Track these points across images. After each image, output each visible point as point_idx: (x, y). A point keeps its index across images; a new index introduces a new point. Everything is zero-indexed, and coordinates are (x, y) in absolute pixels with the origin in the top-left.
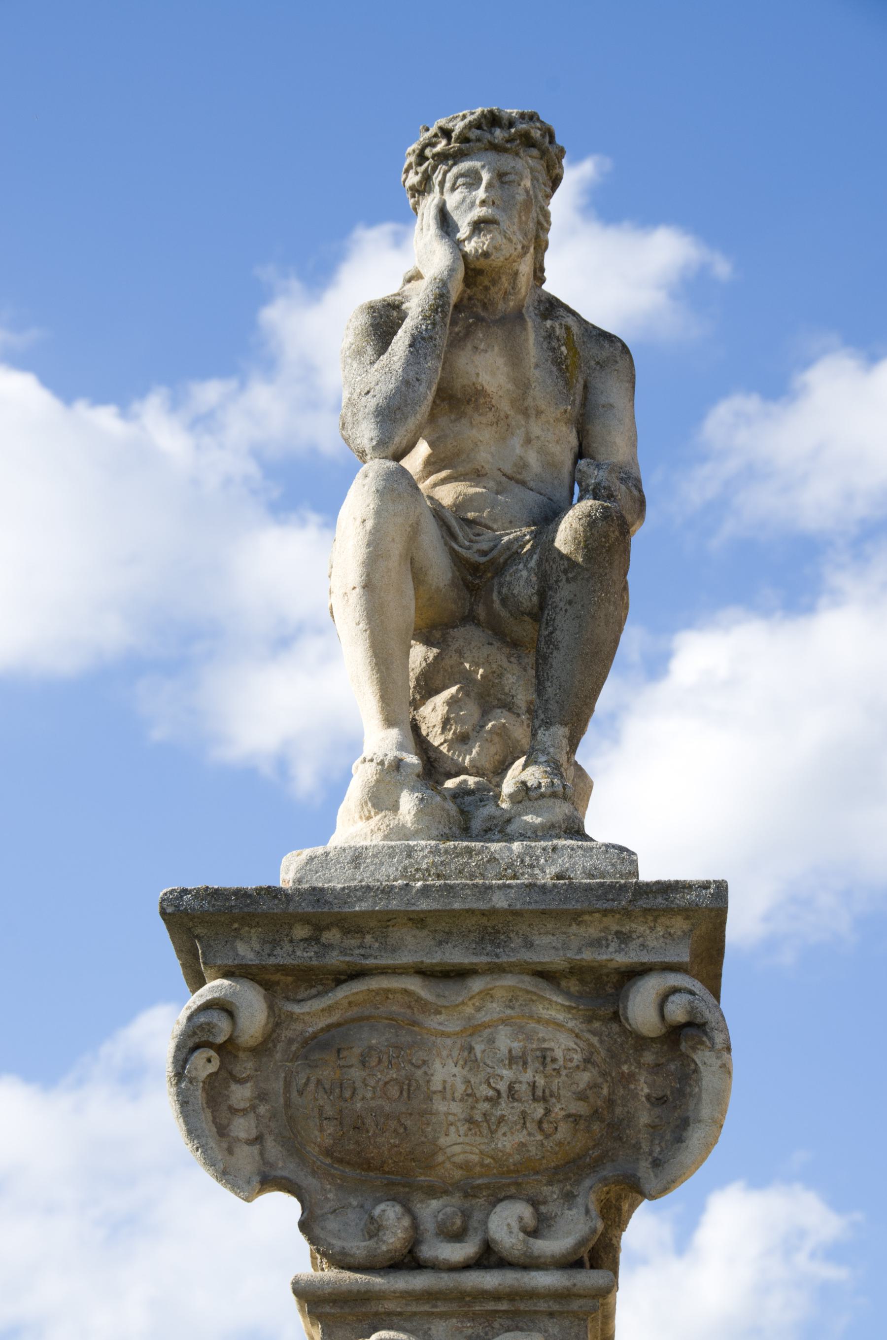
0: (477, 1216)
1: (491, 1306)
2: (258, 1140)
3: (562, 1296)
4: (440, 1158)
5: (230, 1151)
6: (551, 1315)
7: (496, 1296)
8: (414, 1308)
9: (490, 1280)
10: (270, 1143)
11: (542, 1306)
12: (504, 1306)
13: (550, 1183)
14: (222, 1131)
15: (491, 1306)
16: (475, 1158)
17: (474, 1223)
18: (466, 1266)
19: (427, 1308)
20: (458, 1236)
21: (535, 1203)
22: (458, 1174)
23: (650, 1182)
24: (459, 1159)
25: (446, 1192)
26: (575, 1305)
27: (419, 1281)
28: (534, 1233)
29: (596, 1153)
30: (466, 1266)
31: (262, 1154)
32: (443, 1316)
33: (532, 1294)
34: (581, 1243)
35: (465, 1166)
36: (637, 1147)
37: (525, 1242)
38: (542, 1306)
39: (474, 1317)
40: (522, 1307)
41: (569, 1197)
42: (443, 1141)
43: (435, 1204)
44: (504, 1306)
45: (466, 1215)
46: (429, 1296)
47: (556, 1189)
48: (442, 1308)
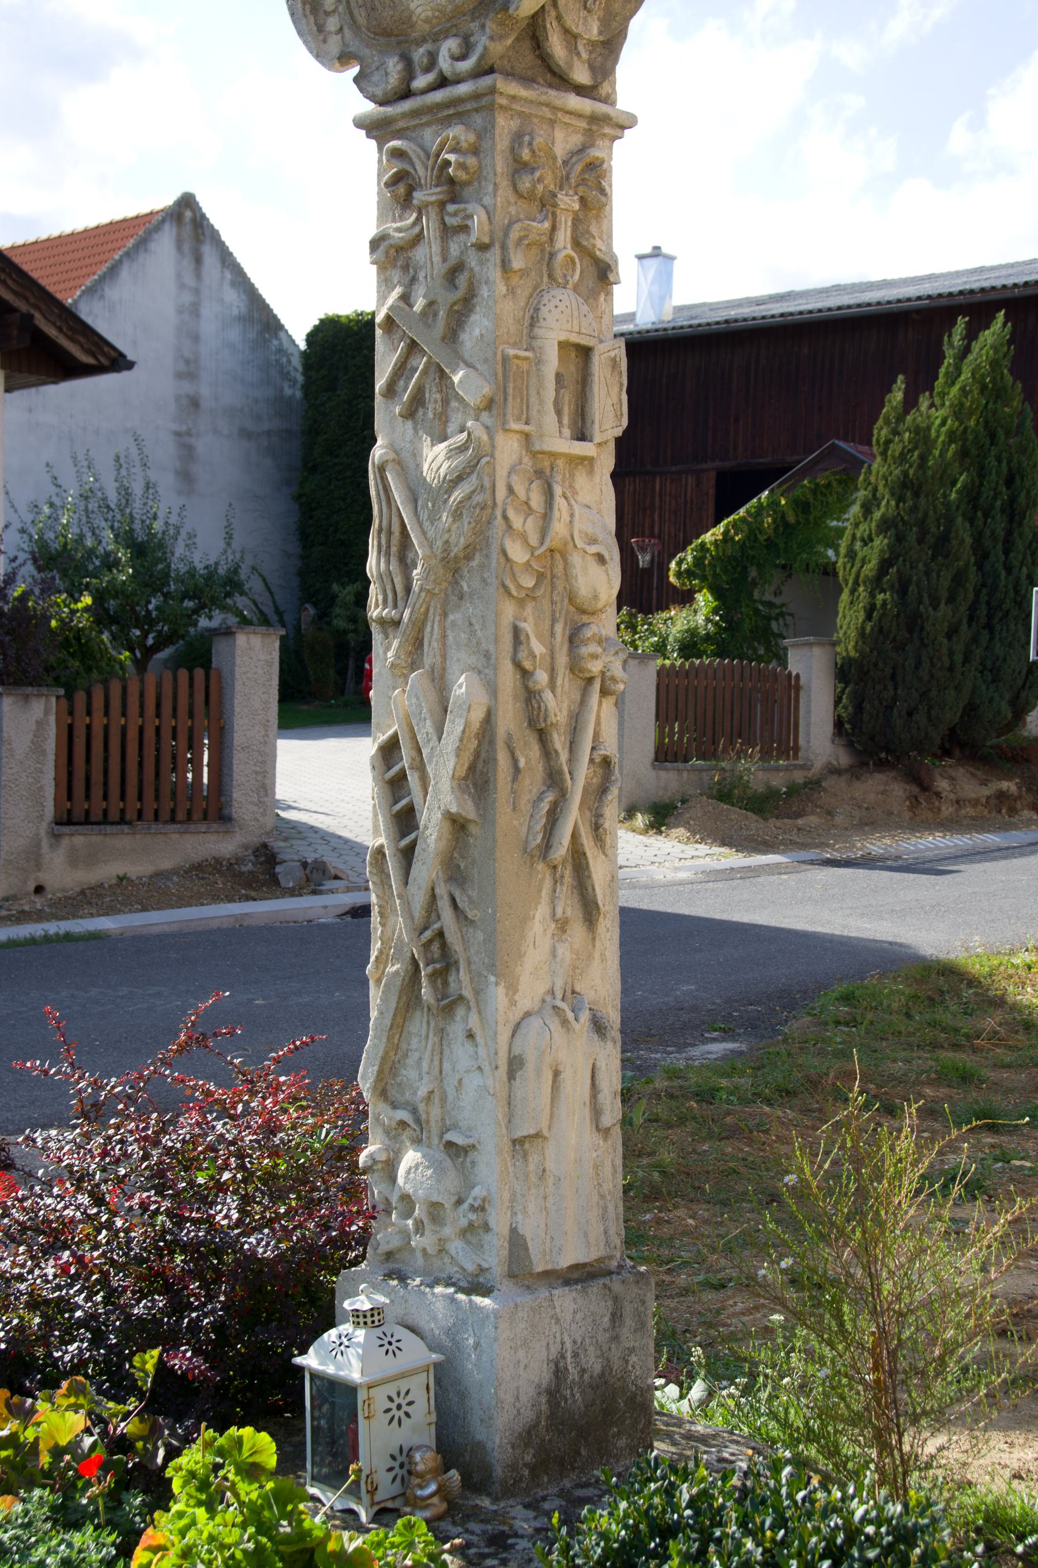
1: (446, 113)
2: (341, 30)
3: (476, 96)
4: (414, 19)
5: (325, 41)
6: (477, 110)
10: (346, 30)
11: (469, 106)
12: (451, 111)
13: (473, 20)
14: (320, 28)
15: (446, 113)
16: (429, 13)
19: (417, 122)
24: (423, 16)
26: (484, 101)
31: (343, 38)
32: (428, 124)
35: (427, 21)
37: (452, 65)
38: (469, 106)
40: (460, 109)
42: (412, 6)
44: (451, 111)
46: (415, 113)
47: (477, 24)
48: (424, 119)
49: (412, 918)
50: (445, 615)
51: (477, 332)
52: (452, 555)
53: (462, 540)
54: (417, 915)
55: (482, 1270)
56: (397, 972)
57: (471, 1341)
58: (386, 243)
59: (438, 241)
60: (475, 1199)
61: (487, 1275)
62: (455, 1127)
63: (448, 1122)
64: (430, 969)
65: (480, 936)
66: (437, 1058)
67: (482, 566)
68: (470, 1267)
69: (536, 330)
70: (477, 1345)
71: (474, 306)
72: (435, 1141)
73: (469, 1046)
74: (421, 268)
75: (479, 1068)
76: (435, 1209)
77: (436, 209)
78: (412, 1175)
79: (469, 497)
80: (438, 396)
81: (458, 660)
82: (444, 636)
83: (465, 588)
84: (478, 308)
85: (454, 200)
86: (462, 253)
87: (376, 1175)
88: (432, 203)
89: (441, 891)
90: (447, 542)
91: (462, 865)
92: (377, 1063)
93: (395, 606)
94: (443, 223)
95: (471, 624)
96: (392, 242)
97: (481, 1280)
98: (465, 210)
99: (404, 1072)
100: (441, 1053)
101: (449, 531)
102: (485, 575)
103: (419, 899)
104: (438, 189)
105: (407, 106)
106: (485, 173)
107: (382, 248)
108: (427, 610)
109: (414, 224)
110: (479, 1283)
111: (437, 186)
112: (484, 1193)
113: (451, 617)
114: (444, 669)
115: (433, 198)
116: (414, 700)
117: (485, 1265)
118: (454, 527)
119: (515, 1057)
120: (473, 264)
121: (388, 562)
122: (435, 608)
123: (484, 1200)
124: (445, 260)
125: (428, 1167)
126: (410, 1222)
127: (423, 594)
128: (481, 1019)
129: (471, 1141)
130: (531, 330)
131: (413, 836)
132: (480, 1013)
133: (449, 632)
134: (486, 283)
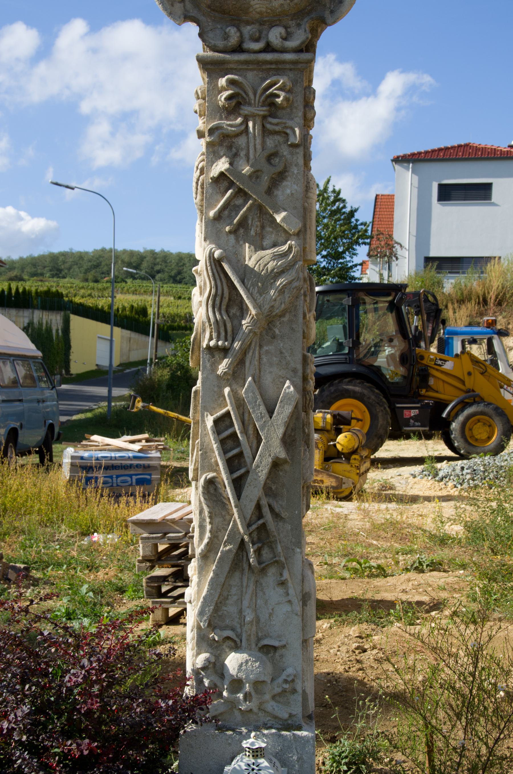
0: (265, 32)
1: (268, 66)
3: (295, 63)
4: (251, 10)
6: (291, 70)
7: (271, 63)
8: (240, 67)
9: (269, 56)
11: (288, 66)
12: (273, 66)
13: (292, 20)
15: (268, 66)
16: (264, 10)
17: (263, 35)
18: (260, 51)
19: (245, 67)
20: (257, 40)
21: (286, 27)
22: (258, 16)
23: (329, 19)
24: (258, 10)
25: (253, 23)
26: (299, 66)
27: (243, 57)
28: (285, 39)
29: (310, 8)
30: (260, 51)
31: (184, 7)
32: (251, 70)
33: (284, 62)
34: (303, 43)
35: (260, 13)
36: (325, 5)
37: (282, 42)
38: (288, 66)
39: (263, 70)
40: (280, 67)
41: (299, 25)
42: (252, 3)
43: (249, 28)
44: (273, 66)
45: (260, 32)
46: (246, 62)
47: (294, 22)
48: (251, 67)
49: (245, 518)
50: (261, 346)
51: (288, 191)
52: (274, 313)
53: (283, 306)
54: (167, 518)
55: (291, 716)
56: (230, 550)
57: (295, 758)
58: (220, 131)
59: (260, 137)
60: (288, 676)
61: (294, 719)
62: (267, 636)
63: (260, 634)
64: (256, 546)
65: (289, 527)
66: (254, 598)
67: (291, 321)
68: (286, 716)
69: (309, 193)
70: (299, 759)
71: (286, 177)
72: (254, 646)
73: (280, 590)
74: (242, 149)
75: (290, 602)
76: (257, 684)
77: (261, 119)
78: (244, 668)
79: (290, 283)
80: (259, 223)
81: (270, 372)
82: (260, 358)
83: (277, 332)
84: (289, 178)
85: (273, 115)
86: (276, 146)
87: (209, 670)
88: (259, 115)
89: (264, 502)
90: (273, 307)
91: (274, 488)
92: (213, 604)
93: (226, 340)
94: (263, 126)
95: (281, 353)
96: (224, 131)
97: (290, 722)
98: (285, 123)
99: (225, 608)
100: (256, 596)
101: (275, 300)
102: (294, 326)
103: (250, 507)
104: (264, 108)
105: (237, 57)
106: (296, 105)
107: (217, 133)
108: (251, 344)
109: (241, 124)
110: (289, 724)
111: (262, 106)
112: (295, 672)
113: (265, 348)
114: (260, 377)
115: (262, 113)
116: (250, 394)
117: (294, 713)
118: (278, 299)
119: (306, 593)
120: (285, 153)
121: (220, 314)
122: (256, 342)
123: (295, 676)
124: (263, 149)
125: (256, 661)
126: (241, 696)
127: (251, 334)
128: (290, 573)
129: (283, 643)
130: (307, 194)
131: (242, 471)
132: (289, 571)
133: (263, 356)
134: (296, 165)
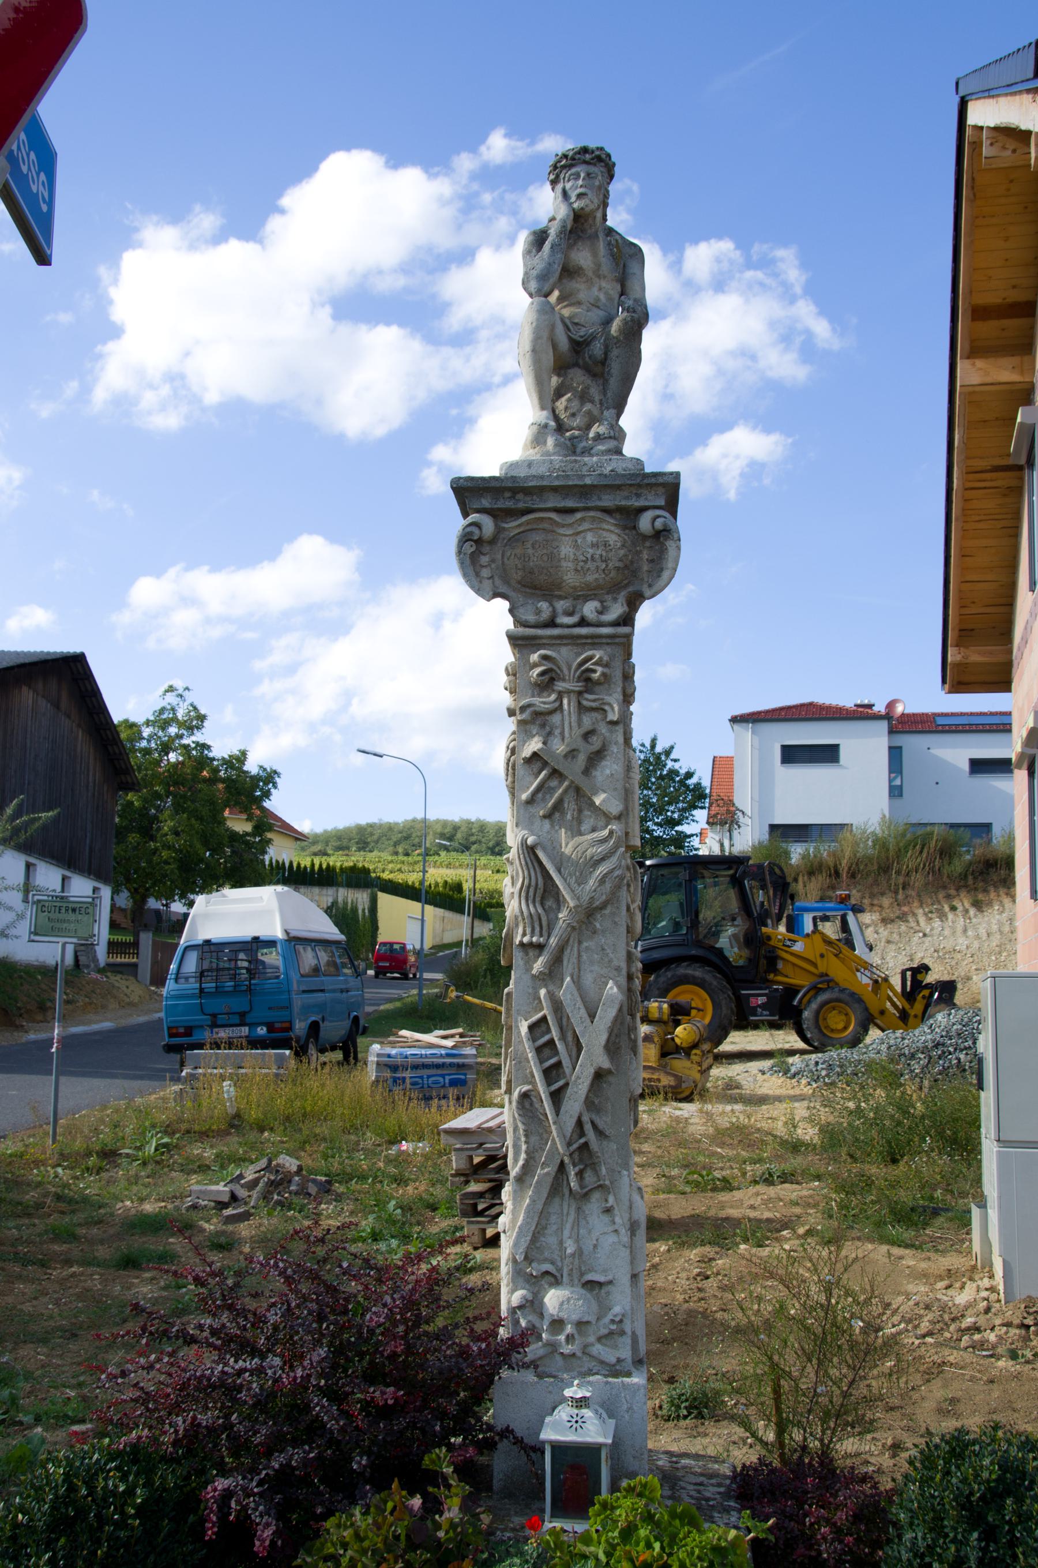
0: (579, 607)
1: (584, 641)
2: (492, 577)
5: (481, 582)
6: (608, 644)
7: (586, 637)
8: (554, 642)
9: (584, 631)
10: (496, 579)
11: (604, 641)
12: (589, 641)
13: (608, 593)
14: (477, 574)
15: (584, 641)
17: (577, 609)
18: (574, 626)
20: (571, 614)
21: (602, 602)
22: (571, 590)
23: (647, 592)
25: (566, 598)
27: (556, 632)
28: (600, 613)
29: (626, 582)
30: (574, 626)
32: (565, 645)
33: (600, 636)
34: (620, 617)
36: (642, 579)
39: (578, 645)
41: (615, 599)
42: (565, 578)
43: (562, 602)
44: (589, 641)
45: (574, 607)
48: (565, 642)
49: (564, 1136)
50: (580, 943)
51: (608, 772)
56: (547, 1174)
58: (532, 709)
60: (615, 1316)
61: (623, 1364)
63: (583, 1269)
64: (577, 1169)
65: (614, 1146)
67: (613, 914)
68: (613, 1360)
71: (605, 756)
72: (576, 1281)
73: (606, 1218)
74: (556, 727)
76: (580, 1325)
78: (565, 1306)
79: (612, 871)
81: (591, 971)
82: (579, 956)
83: (598, 925)
89: (586, 1118)
91: (596, 1102)
92: (530, 1234)
93: (541, 935)
94: (579, 703)
95: (603, 949)
96: (537, 709)
97: (618, 1367)
101: (595, 891)
103: (570, 1124)
107: (528, 711)
109: (555, 701)
113: (585, 944)
115: (577, 689)
117: (623, 1357)
120: (603, 731)
121: (535, 906)
123: (623, 1315)
126: (562, 1338)
129: (610, 1278)
